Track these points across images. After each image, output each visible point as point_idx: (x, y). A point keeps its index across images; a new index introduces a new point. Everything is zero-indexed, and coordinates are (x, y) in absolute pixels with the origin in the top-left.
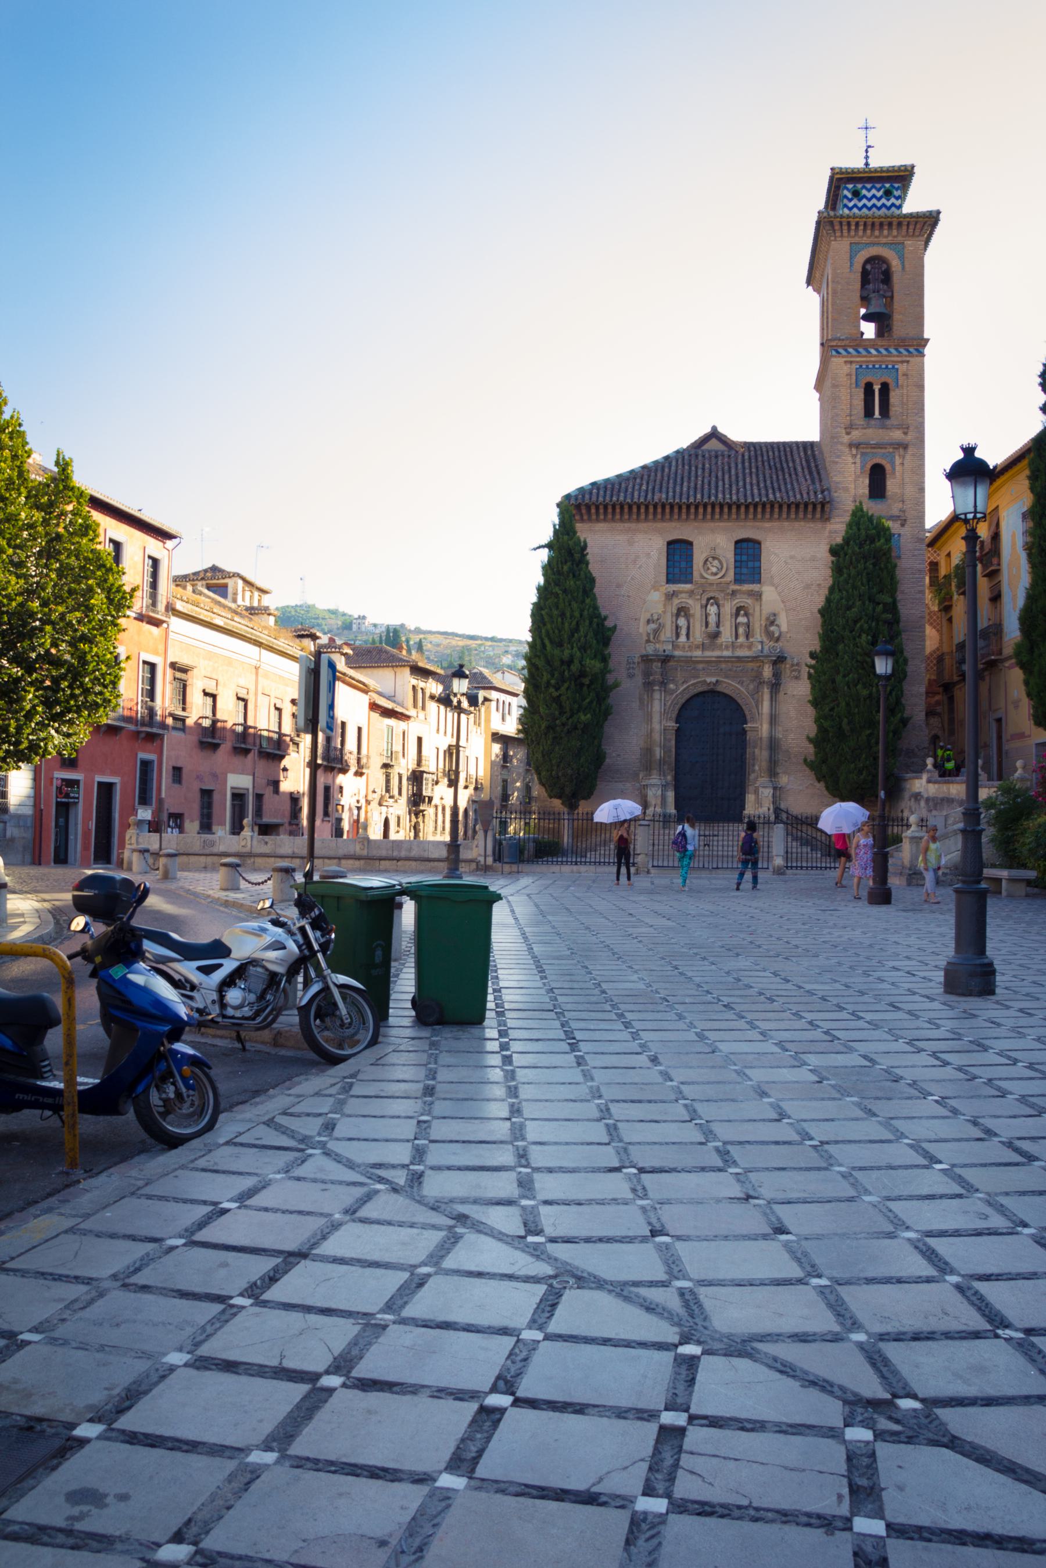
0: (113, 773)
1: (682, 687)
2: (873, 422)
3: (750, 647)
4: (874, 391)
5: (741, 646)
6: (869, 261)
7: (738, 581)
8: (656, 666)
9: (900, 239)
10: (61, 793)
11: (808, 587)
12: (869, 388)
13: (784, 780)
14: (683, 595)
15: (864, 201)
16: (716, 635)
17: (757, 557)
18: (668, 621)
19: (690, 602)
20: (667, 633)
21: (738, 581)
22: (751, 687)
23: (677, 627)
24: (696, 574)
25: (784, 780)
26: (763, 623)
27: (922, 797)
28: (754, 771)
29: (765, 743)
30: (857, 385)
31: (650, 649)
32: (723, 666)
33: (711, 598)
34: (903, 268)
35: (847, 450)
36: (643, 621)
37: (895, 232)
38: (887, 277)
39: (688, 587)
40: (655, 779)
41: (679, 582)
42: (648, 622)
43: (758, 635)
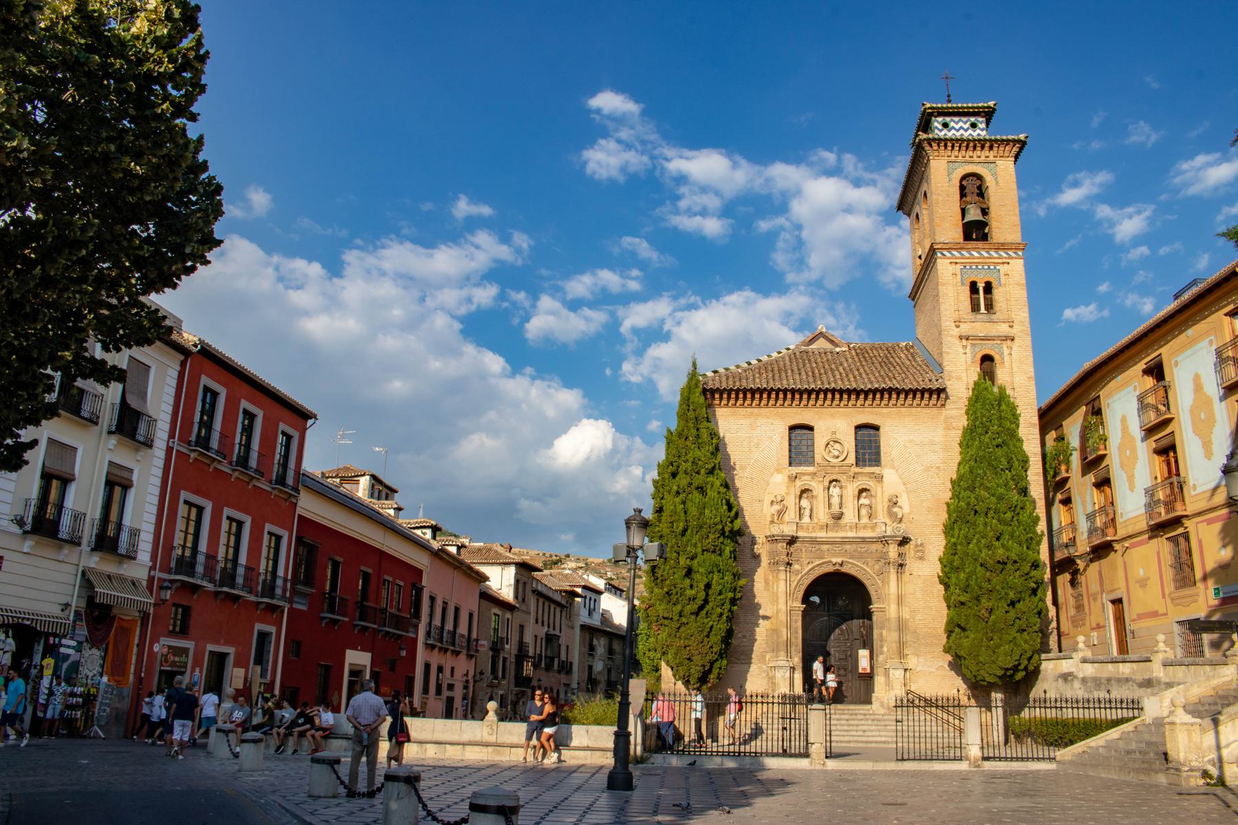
0: (227, 643)
1: (808, 568)
2: (979, 316)
3: (874, 527)
5: (865, 527)
6: (964, 178)
8: (781, 546)
9: (991, 158)
10: (166, 661)
11: (927, 469)
12: (973, 288)
13: (912, 662)
14: (806, 477)
15: (953, 131)
16: (839, 517)
18: (791, 502)
19: (813, 484)
20: (791, 515)
22: (877, 567)
24: (818, 458)
25: (912, 662)
26: (886, 504)
27: (1076, 677)
28: (882, 653)
29: (894, 624)
30: (963, 284)
31: (775, 530)
32: (848, 547)
33: (831, 482)
34: (997, 183)
35: (957, 341)
36: (767, 502)
38: (981, 193)
39: (811, 469)
40: (782, 661)
41: (800, 464)
42: (772, 502)
43: (882, 517)
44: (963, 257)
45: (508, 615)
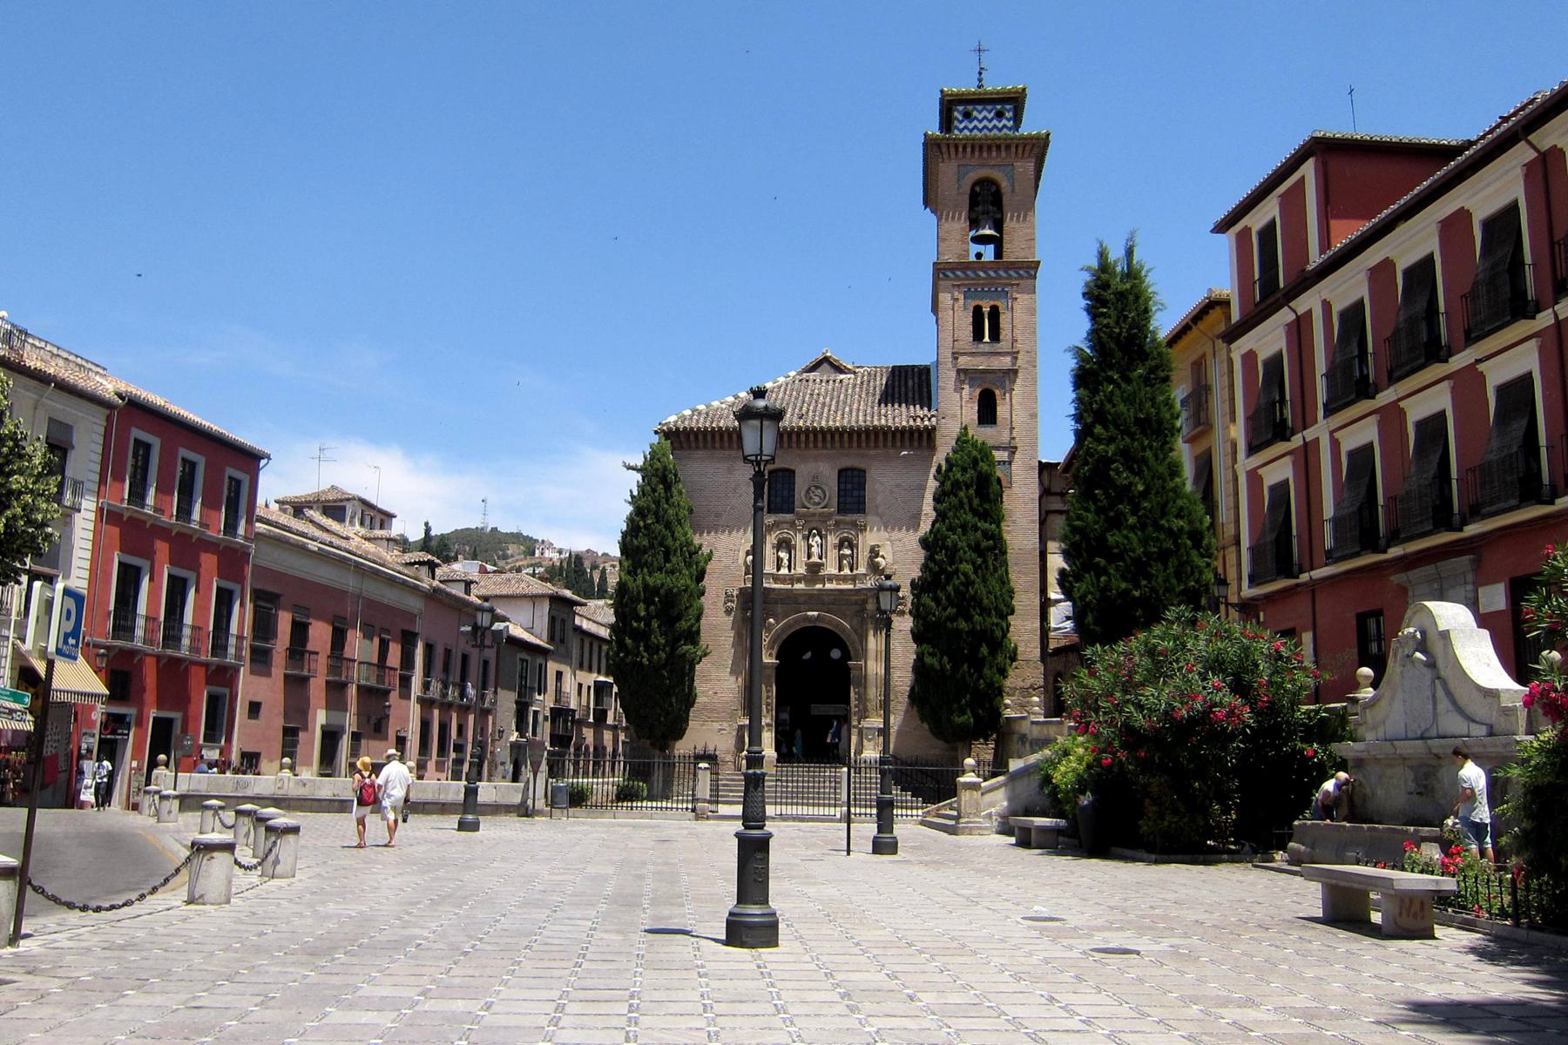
2: (982, 348)
4: (982, 315)
5: (845, 579)
7: (839, 511)
17: (861, 486)
21: (839, 511)
23: (779, 560)
26: (867, 554)
37: (1003, 154)
38: (997, 199)
39: (789, 517)
44: (968, 277)
45: (540, 660)
